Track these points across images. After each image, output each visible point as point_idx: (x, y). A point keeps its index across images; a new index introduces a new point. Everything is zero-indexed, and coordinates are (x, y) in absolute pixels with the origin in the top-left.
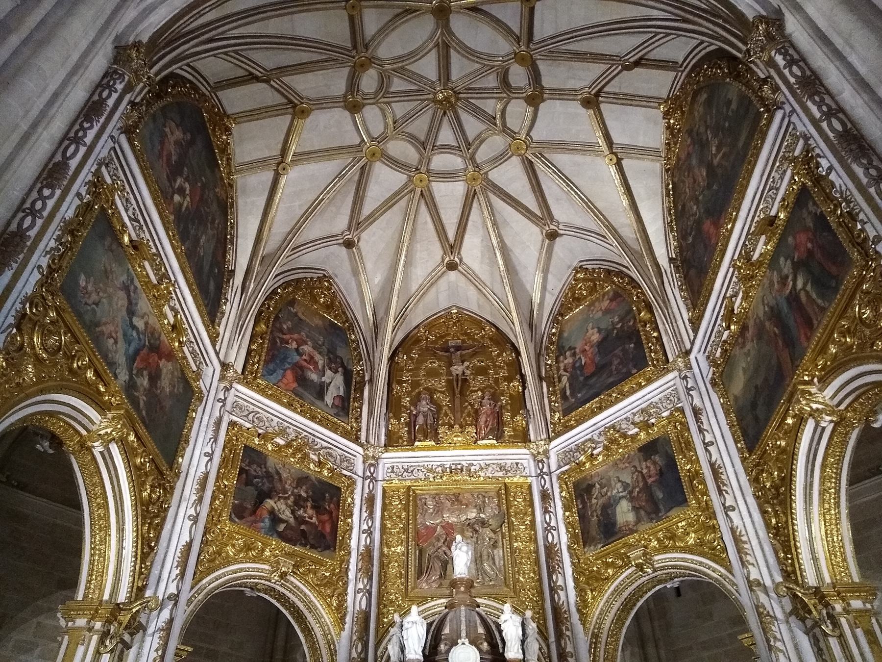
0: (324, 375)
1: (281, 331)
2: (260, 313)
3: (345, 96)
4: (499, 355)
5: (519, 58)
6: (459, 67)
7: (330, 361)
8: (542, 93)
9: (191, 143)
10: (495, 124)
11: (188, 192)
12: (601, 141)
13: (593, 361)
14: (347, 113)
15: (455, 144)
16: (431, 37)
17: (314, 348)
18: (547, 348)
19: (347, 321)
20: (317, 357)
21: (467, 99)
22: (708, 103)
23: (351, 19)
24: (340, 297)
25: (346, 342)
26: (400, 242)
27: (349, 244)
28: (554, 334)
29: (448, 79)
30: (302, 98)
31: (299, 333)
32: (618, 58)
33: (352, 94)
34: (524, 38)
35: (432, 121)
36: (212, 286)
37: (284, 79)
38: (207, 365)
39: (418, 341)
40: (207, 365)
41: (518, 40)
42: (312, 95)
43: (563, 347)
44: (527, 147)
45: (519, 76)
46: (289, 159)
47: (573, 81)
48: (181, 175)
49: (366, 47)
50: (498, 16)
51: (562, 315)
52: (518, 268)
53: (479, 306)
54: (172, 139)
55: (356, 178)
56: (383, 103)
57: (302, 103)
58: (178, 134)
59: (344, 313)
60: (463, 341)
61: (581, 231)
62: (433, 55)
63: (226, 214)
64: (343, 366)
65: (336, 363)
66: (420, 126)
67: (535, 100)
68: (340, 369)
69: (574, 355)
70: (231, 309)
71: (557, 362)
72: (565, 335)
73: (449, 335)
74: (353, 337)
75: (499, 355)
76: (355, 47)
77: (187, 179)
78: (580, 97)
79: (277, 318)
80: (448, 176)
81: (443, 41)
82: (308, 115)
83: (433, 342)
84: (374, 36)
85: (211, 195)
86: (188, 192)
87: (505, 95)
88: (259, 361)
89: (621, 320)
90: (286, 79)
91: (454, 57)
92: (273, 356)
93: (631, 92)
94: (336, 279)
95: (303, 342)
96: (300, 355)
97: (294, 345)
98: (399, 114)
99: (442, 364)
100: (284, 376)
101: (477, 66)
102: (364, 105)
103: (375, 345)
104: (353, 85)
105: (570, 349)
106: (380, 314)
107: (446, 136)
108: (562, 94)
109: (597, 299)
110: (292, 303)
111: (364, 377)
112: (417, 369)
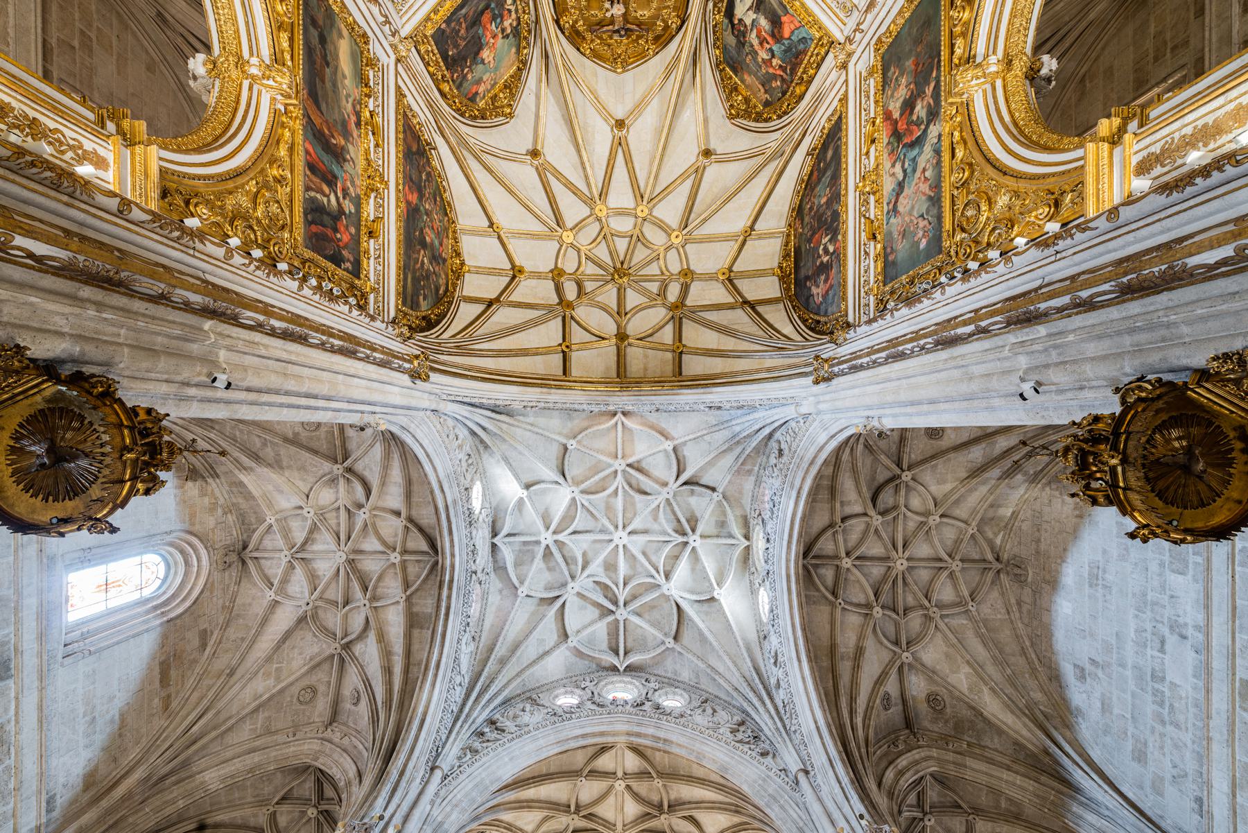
0: (754, 21)
1: (783, 80)
2: (798, 102)
4: (576, 22)
5: (570, 305)
6: (609, 296)
7: (744, 34)
9: (807, 278)
11: (822, 247)
12: (505, 240)
13: (485, 28)
15: (615, 238)
17: (756, 53)
18: (529, 32)
19: (721, 71)
20: (755, 42)
22: (437, 289)
23: (680, 341)
24: (724, 96)
25: (725, 49)
26: (662, 155)
27: (707, 153)
28: (525, 48)
31: (767, 72)
34: (568, 319)
35: (631, 259)
36: (830, 154)
37: (733, 301)
38: (861, 73)
39: (657, 39)
40: (861, 73)
41: (572, 318)
43: (514, 36)
44: (561, 237)
45: (571, 292)
46: (742, 238)
48: (822, 262)
51: (519, 69)
52: (563, 122)
53: (596, 75)
54: (819, 290)
55: (693, 216)
58: (814, 290)
59: (722, 80)
60: (611, 38)
61: (510, 157)
63: (800, 206)
64: (733, 25)
65: (739, 32)
66: (641, 254)
67: (557, 275)
68: (736, 22)
69: (503, 30)
70: (821, 121)
71: (518, 19)
72: (514, 50)
73: (625, 45)
74: (717, 52)
75: (576, 22)
76: (681, 318)
77: (819, 256)
79: (784, 93)
80: (621, 212)
83: (639, 37)
85: (806, 230)
86: (822, 247)
88: (811, 56)
89: (465, 77)
90: (733, 301)
92: (797, 58)
94: (724, 113)
95: (768, 63)
96: (771, 51)
97: (775, 62)
98: (655, 265)
99: (633, 14)
100: (792, 32)
103: (698, 42)
104: (685, 289)
105: (507, 36)
106: (689, 76)
107: (621, 245)
108: (538, 275)
109: (489, 91)
110: (767, 104)
111: (715, 6)
112: (659, 9)
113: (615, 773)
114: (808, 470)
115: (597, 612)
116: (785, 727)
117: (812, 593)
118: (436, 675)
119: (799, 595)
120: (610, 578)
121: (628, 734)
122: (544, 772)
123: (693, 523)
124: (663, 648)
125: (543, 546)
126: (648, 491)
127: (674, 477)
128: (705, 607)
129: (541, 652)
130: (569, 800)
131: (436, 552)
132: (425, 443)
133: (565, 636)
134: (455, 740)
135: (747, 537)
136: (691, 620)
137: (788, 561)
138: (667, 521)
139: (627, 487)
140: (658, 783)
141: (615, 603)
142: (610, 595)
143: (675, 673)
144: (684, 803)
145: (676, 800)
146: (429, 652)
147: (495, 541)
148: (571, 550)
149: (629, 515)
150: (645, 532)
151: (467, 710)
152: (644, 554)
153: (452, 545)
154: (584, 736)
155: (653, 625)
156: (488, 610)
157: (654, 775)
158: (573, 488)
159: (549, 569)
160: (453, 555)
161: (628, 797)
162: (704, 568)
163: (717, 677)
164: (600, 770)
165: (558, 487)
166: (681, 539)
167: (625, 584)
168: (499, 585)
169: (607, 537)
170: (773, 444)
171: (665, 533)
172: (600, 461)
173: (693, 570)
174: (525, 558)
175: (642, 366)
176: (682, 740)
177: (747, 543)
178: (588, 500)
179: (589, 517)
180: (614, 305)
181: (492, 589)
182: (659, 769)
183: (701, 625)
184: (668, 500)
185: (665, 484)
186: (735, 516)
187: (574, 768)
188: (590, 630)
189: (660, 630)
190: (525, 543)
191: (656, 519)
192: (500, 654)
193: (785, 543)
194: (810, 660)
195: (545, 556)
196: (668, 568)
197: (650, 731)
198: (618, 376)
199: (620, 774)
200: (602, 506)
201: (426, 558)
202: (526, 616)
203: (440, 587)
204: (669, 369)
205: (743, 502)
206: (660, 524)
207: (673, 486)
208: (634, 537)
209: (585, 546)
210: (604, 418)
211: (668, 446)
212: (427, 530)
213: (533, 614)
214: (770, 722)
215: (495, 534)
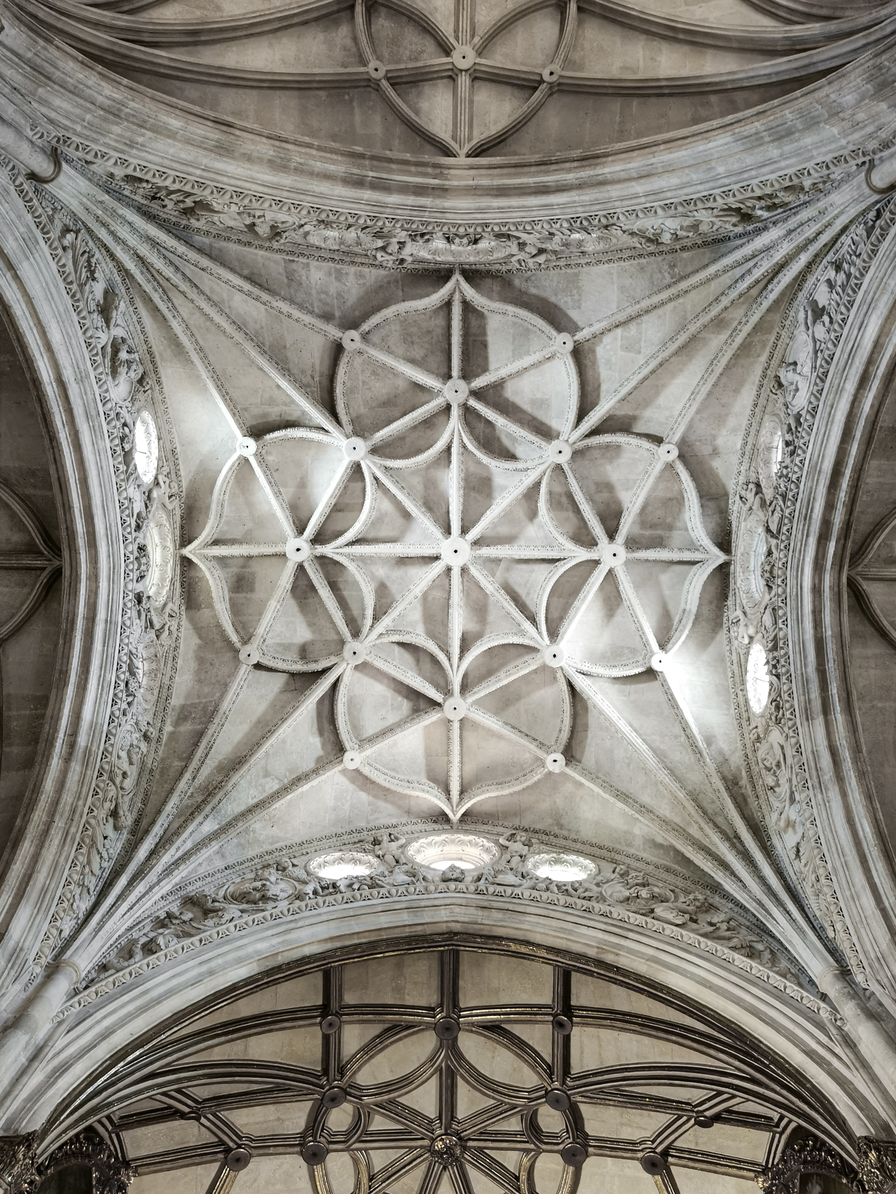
3: (303, 1135)
5: (555, 1103)
8: (586, 1146)
10: (518, 1189)
14: (304, 1165)
16: (432, 1059)
21: (481, 1150)
23: (326, 1039)
29: (453, 1117)
30: (240, 1138)
32: (689, 1108)
33: (314, 1136)
34: (558, 1069)
37: (223, 1114)
42: (256, 1132)
47: (630, 1130)
49: (342, 1071)
50: (523, 1037)
56: (357, 1149)
57: (239, 1146)
62: (433, 1083)
76: (326, 1071)
78: (640, 1155)
81: (448, 1067)
82: (246, 1164)
84: (354, 1056)
87: (532, 1146)
90: (223, 1114)
91: (461, 1085)
93: (712, 1149)
101: (492, 1102)
102: (328, 1151)
104: (316, 1122)
113: (475, 79)
114: (52, 814)
115: (510, 392)
116: (90, 231)
117: (39, 492)
118: (871, 362)
119: (68, 507)
120: (479, 462)
121: (443, 191)
122: (635, 102)
123: (303, 582)
124: (365, 327)
125: (621, 538)
126: (397, 648)
127: (342, 690)
128: (274, 413)
129: (633, 328)
130: (580, 23)
131: (851, 583)
132: (868, 901)
133: (578, 354)
134: (836, 217)
135: (186, 563)
136: (303, 387)
137: (94, 577)
138: (356, 583)
139: (441, 657)
140: (376, 68)
141: (468, 412)
142: (481, 426)
143: (339, 275)
144: (316, 19)
145: (337, 23)
146: (881, 404)
147: (722, 558)
148: (559, 524)
149: (438, 594)
150: (403, 561)
151: (804, 259)
152: (407, 515)
153: (817, 613)
154: (543, 190)
155: (392, 370)
156: (745, 422)
157: (385, 84)
158: (554, 664)
159: (609, 487)
160: (817, 590)
161: (446, 28)
162: (278, 494)
163: (247, 286)
164: (508, 90)
165: (585, 668)
166: (328, 550)
167: (449, 449)
168: (717, 464)
169: (486, 551)
170: (127, 819)
171: (363, 560)
172: (496, 713)
173: (303, 485)
174: (659, 513)
175: (407, 971)
176: (323, 187)
177: (187, 551)
178: (523, 633)
179: (522, 592)
180: (463, 1089)
181: (735, 459)
182: (374, 95)
183: (284, 384)
184: (356, 633)
185: (364, 667)
186: (211, 606)
187: (567, 99)
188: (526, 361)
189: (371, 361)
190: (658, 543)
191: (382, 591)
192: (724, 336)
193: (101, 615)
194: (36, 383)
195: (618, 514)
196: (359, 485)
197: (393, 199)
198: (456, 954)
199: (464, 81)
200: (492, 616)
201: (874, 571)
202: (661, 400)
203: (847, 526)
204: (350, 975)
205: (195, 641)
206: (373, 577)
207: (345, 669)
208: (428, 551)
209: (531, 530)
210: (486, 808)
211: (354, 758)
212: (870, 630)
213: (647, 403)
214: (123, 232)
215: (723, 573)
